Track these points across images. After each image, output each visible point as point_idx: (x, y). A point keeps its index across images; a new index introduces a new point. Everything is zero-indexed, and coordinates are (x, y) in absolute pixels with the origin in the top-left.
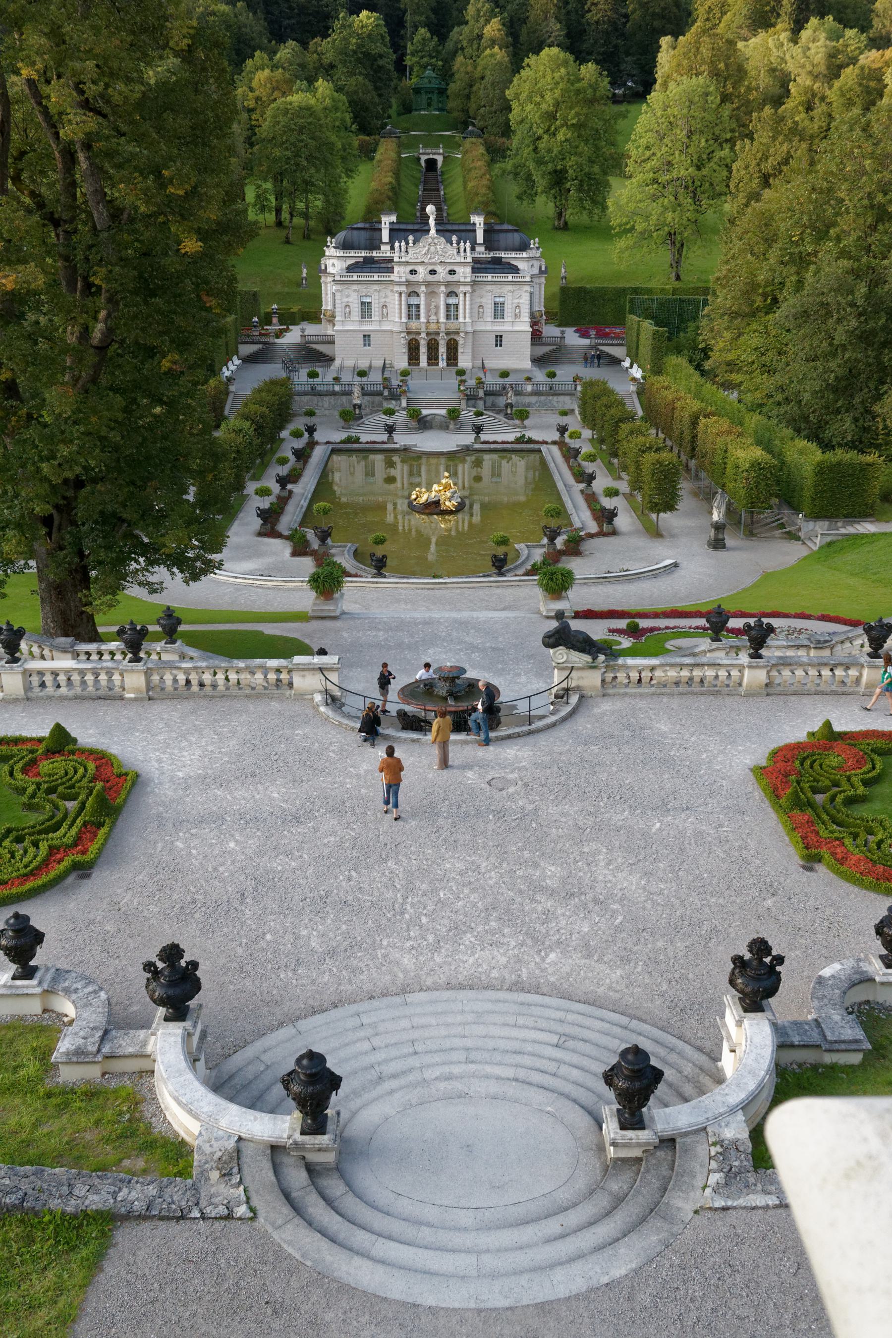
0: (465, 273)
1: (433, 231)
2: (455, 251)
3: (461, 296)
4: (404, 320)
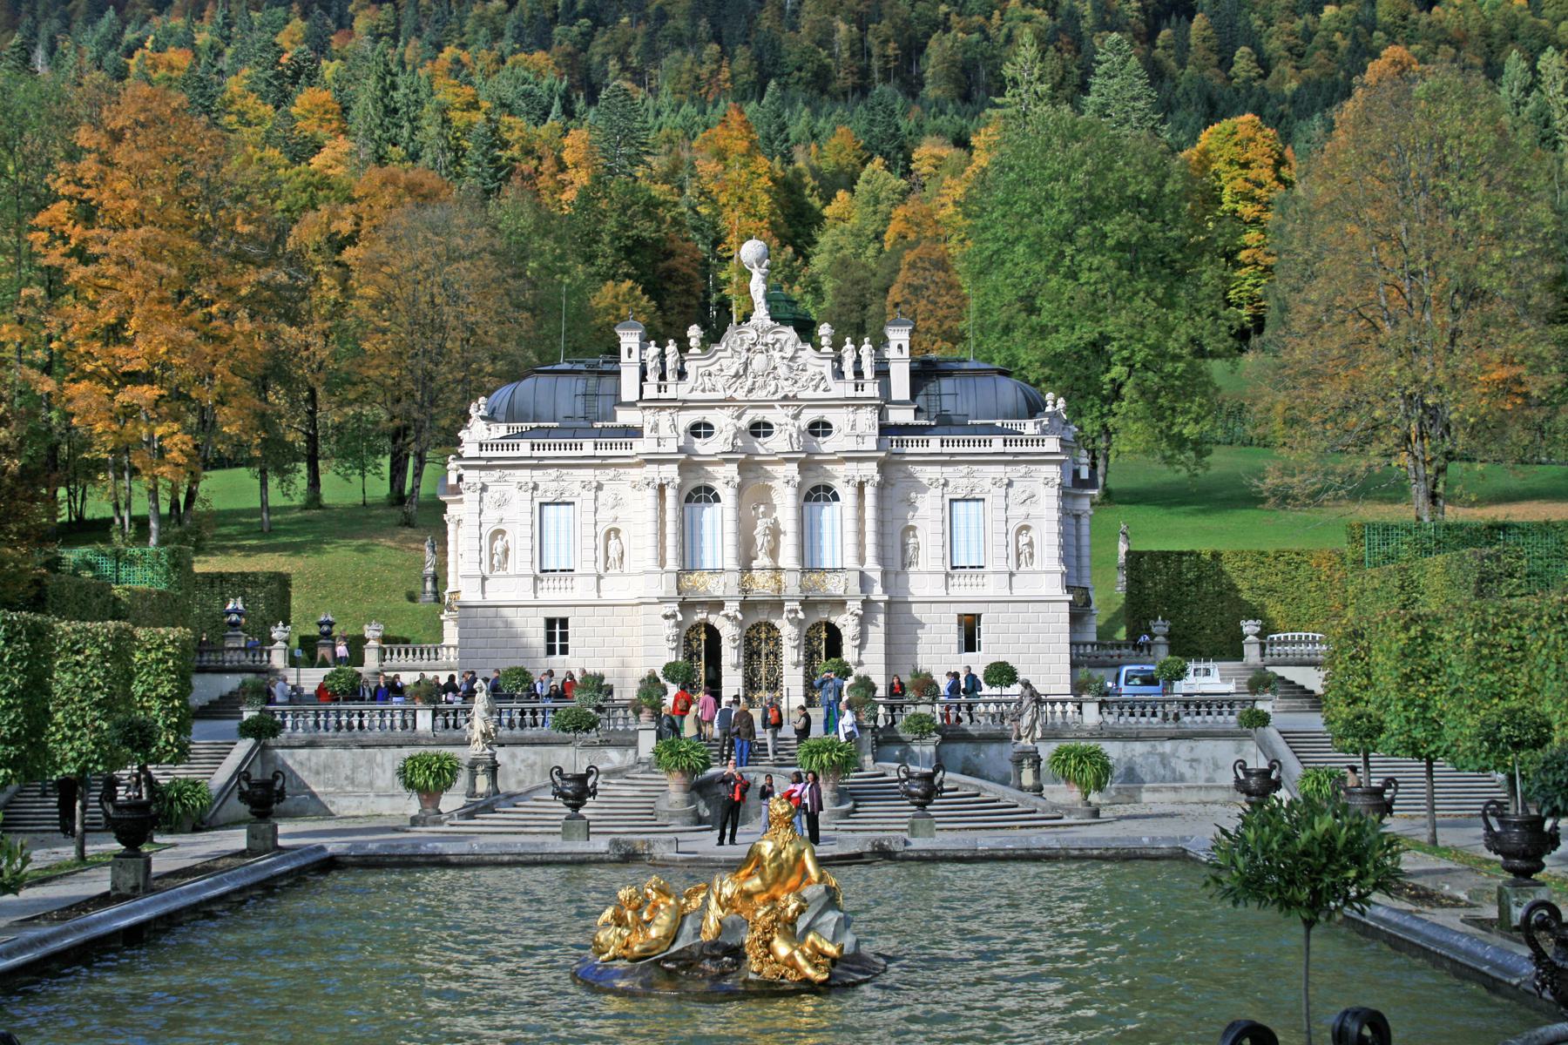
0: (854, 430)
1: (761, 314)
2: (827, 368)
3: (847, 494)
4: (672, 564)
